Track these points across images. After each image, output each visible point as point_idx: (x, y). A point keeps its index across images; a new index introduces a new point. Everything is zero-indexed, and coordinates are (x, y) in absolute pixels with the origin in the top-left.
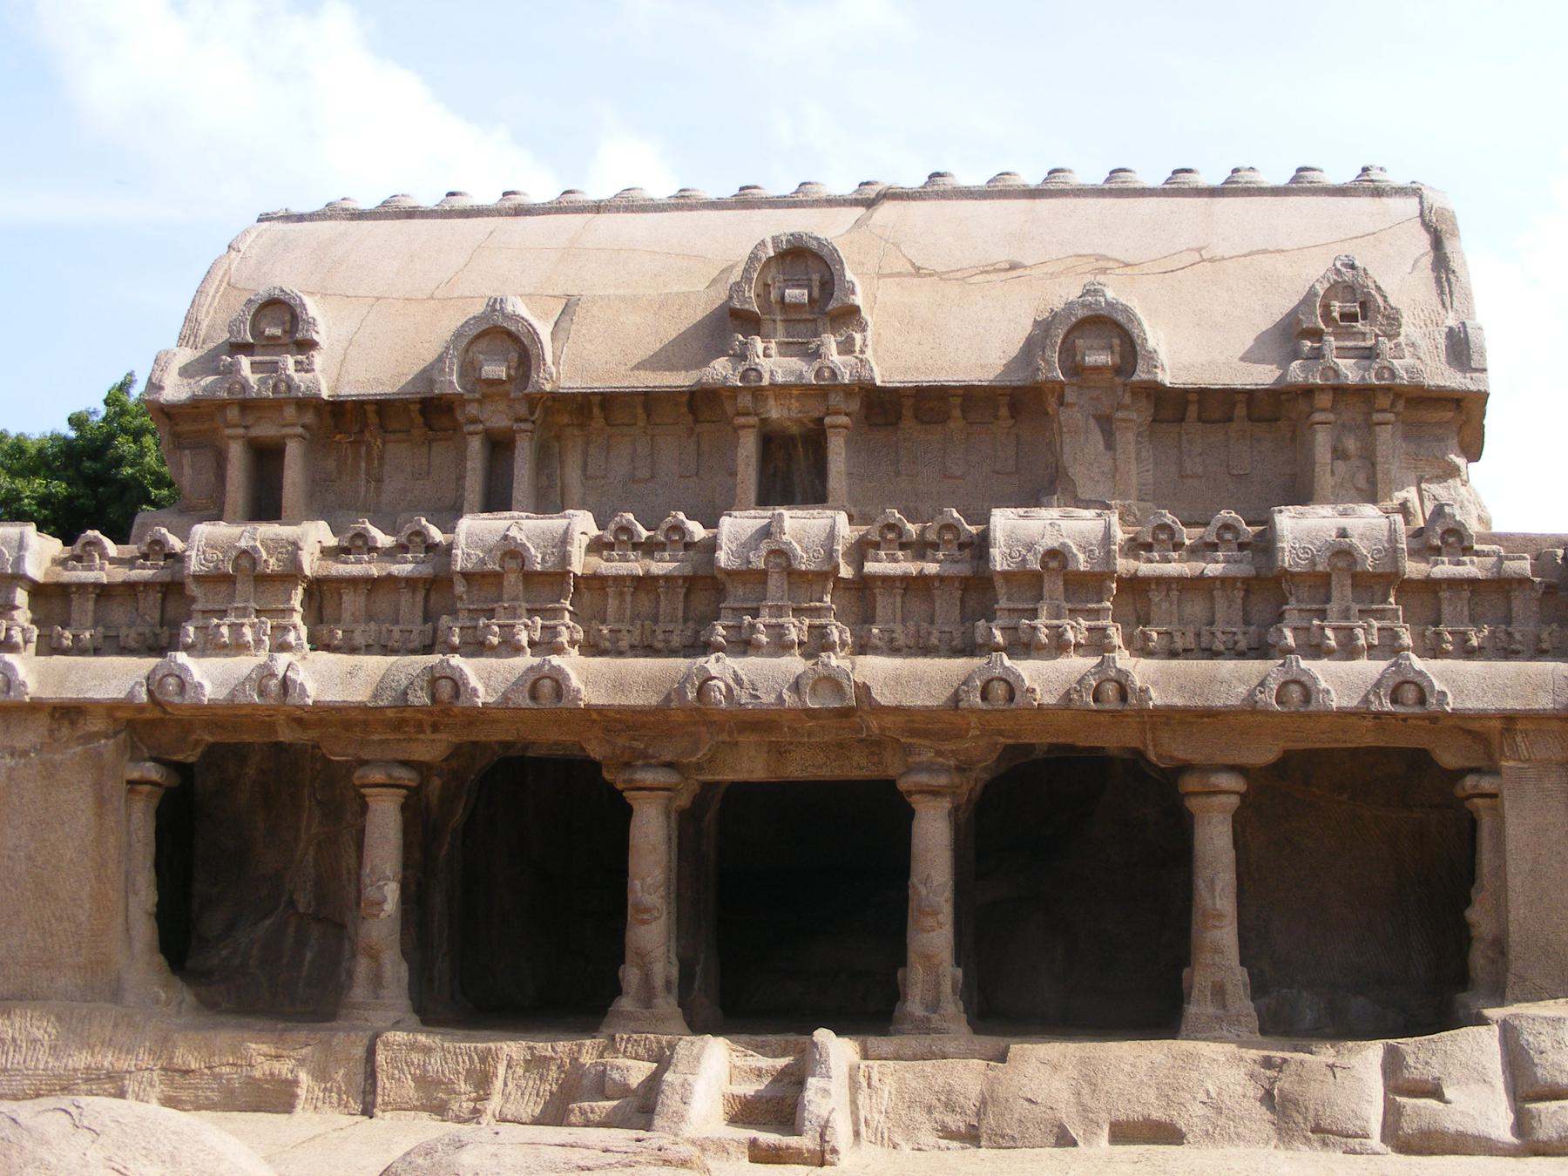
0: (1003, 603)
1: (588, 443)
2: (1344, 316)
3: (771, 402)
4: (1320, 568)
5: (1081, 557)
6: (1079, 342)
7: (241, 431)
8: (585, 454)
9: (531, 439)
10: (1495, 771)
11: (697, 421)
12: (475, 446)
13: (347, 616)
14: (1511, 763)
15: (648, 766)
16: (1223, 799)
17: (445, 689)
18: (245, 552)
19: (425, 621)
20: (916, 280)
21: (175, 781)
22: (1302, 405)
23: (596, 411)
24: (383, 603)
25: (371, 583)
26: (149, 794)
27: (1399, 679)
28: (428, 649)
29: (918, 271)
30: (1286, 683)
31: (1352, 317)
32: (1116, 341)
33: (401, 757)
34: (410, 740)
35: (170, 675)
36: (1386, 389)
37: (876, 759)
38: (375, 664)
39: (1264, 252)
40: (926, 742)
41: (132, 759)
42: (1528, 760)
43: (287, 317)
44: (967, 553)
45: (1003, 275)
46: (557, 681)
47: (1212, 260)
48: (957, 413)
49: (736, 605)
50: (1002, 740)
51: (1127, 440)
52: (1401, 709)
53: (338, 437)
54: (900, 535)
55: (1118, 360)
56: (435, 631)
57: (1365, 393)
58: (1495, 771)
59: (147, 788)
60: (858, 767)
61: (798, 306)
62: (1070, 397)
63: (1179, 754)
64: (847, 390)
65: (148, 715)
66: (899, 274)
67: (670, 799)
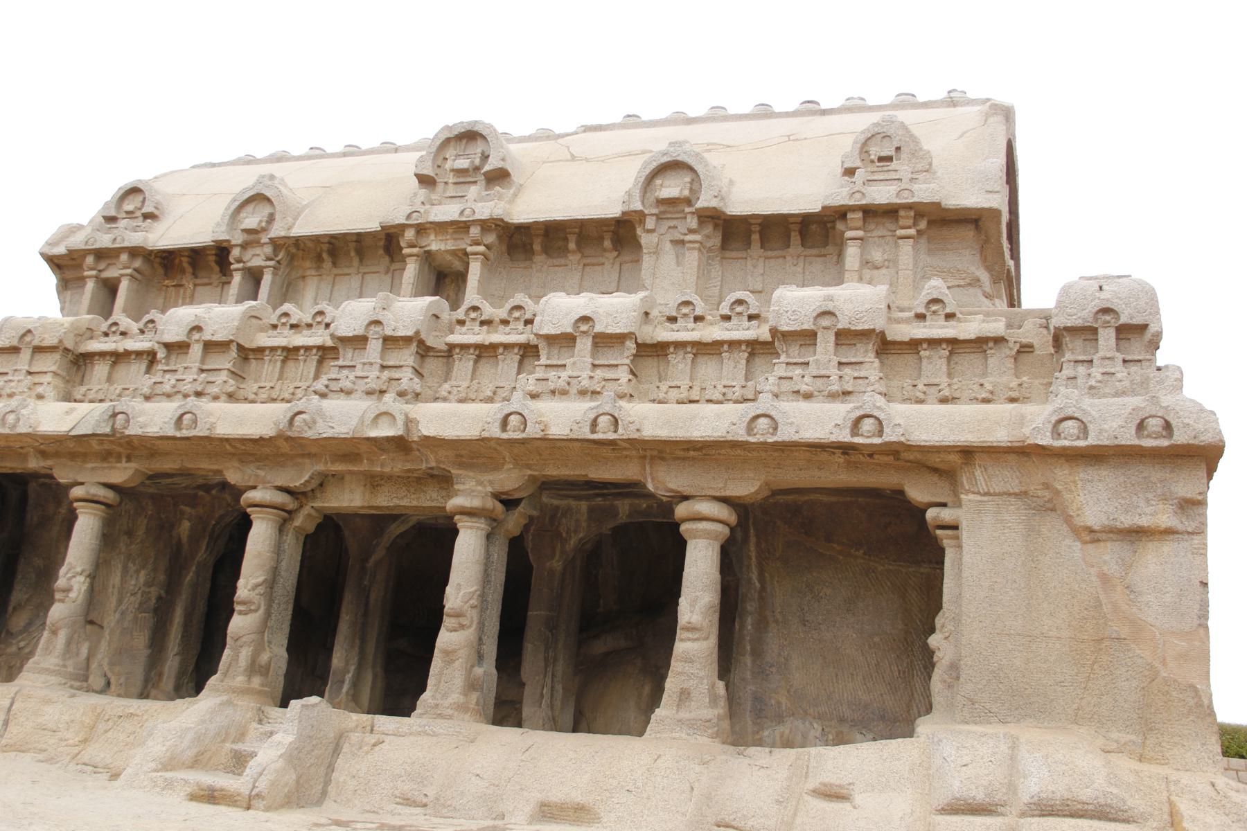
2: (881, 159)
3: (432, 237)
4: (805, 327)
7: (94, 273)
8: (318, 288)
10: (959, 504)
11: (392, 261)
14: (971, 497)
22: (840, 226)
27: (861, 412)
31: (889, 159)
36: (909, 207)
38: (84, 408)
40: (471, 474)
42: (985, 494)
48: (572, 246)
50: (529, 472)
51: (692, 258)
58: (959, 504)
62: (650, 223)
63: (672, 486)
64: (487, 225)
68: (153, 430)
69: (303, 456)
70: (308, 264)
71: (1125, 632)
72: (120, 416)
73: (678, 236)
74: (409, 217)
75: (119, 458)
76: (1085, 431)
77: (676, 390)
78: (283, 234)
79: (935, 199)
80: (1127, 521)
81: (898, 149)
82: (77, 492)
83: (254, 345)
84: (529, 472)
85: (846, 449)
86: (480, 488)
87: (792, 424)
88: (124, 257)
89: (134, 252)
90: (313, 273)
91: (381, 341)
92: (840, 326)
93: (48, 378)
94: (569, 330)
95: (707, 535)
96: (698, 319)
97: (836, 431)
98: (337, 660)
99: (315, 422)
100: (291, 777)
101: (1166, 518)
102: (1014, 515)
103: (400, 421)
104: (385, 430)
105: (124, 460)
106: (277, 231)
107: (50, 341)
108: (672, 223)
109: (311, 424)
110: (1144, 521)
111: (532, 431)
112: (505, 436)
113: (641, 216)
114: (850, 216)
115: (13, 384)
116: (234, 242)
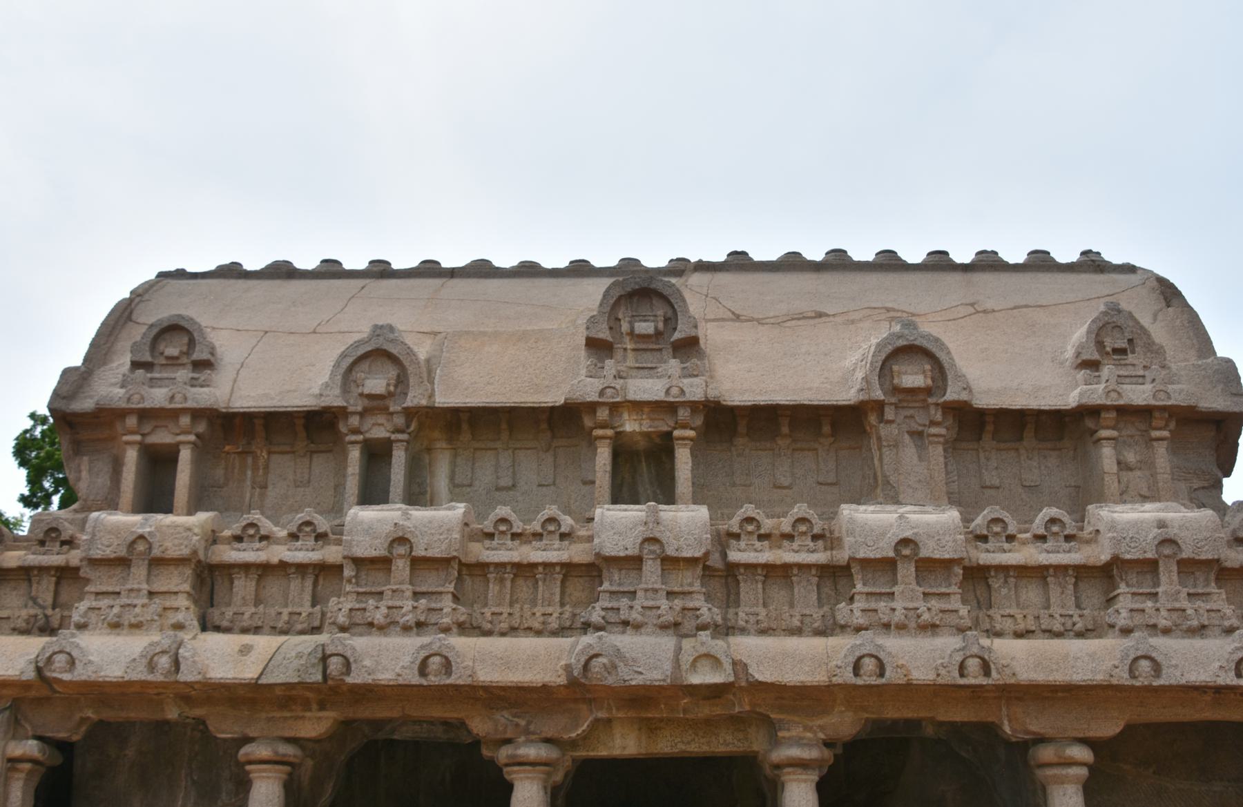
0: (859, 587)
1: (455, 456)
2: (1116, 351)
3: (626, 416)
4: (1149, 555)
5: (931, 543)
6: (895, 368)
7: (138, 438)
8: (453, 465)
9: (406, 450)
11: (554, 437)
12: (355, 454)
13: (237, 599)
15: (529, 742)
16: (1073, 771)
17: (335, 664)
18: (142, 537)
19: (313, 605)
20: (737, 324)
21: (58, 760)
22: (1090, 423)
23: (465, 426)
24: (273, 587)
25: (265, 570)
26: (30, 773)
28: (316, 630)
29: (737, 318)
30: (1136, 659)
32: (928, 367)
33: (288, 734)
34: (297, 718)
35: (60, 652)
36: (1163, 409)
37: (741, 736)
38: (264, 644)
39: (1026, 306)
40: (796, 719)
41: (14, 737)
43: (185, 340)
44: (820, 543)
45: (812, 322)
46: (446, 658)
47: (985, 312)
48: (785, 430)
49: (614, 588)
51: (937, 453)
53: (227, 448)
54: (759, 527)
55: (929, 382)
56: (323, 614)
57: (1145, 413)
59: (27, 766)
60: (724, 743)
62: (889, 413)
63: (1033, 728)
64: (694, 406)
65: (33, 694)
66: (723, 320)
67: (549, 774)
68: (385, 676)
69: (576, 701)
70: (436, 434)
72: (334, 660)
73: (916, 427)
74: (602, 393)
75: (306, 705)
77: (1010, 620)
78: (424, 402)
79: (1192, 402)
81: (1130, 341)
83: (471, 559)
84: (866, 715)
85: (1219, 691)
86: (809, 735)
87: (1176, 666)
88: (185, 420)
89: (197, 414)
90: (444, 445)
91: (659, 561)
92: (1184, 555)
94: (891, 554)
96: (1011, 538)
97: (1222, 674)
99: (615, 667)
103: (728, 667)
105: (315, 706)
106: (416, 398)
108: (911, 412)
112: (859, 682)
113: (879, 406)
114: (1103, 415)
115: (137, 610)
116: (351, 409)
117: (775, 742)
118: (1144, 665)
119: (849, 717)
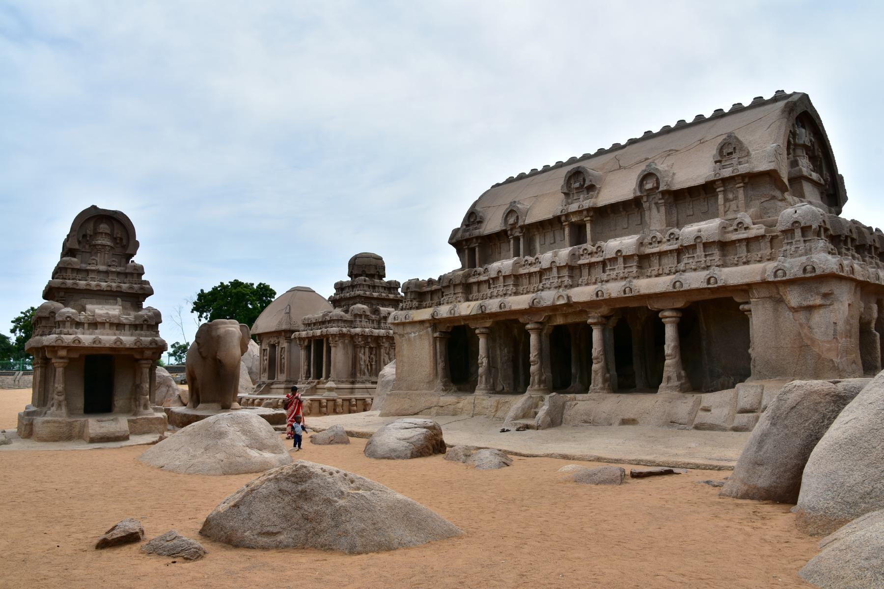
38: (473, 304)
51: (663, 209)
52: (710, 286)
61: (577, 188)
64: (589, 210)
71: (809, 343)
76: (785, 274)
80: (805, 304)
82: (477, 331)
89: (477, 238)
93: (460, 295)
95: (671, 322)
98: (573, 371)
100: (549, 419)
101: (818, 301)
102: (769, 305)
104: (562, 302)
107: (458, 282)
109: (539, 302)
110: (811, 303)
111: (606, 296)
117: (589, 317)
118: (678, 284)
119: (606, 308)
